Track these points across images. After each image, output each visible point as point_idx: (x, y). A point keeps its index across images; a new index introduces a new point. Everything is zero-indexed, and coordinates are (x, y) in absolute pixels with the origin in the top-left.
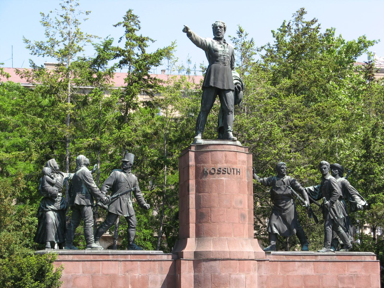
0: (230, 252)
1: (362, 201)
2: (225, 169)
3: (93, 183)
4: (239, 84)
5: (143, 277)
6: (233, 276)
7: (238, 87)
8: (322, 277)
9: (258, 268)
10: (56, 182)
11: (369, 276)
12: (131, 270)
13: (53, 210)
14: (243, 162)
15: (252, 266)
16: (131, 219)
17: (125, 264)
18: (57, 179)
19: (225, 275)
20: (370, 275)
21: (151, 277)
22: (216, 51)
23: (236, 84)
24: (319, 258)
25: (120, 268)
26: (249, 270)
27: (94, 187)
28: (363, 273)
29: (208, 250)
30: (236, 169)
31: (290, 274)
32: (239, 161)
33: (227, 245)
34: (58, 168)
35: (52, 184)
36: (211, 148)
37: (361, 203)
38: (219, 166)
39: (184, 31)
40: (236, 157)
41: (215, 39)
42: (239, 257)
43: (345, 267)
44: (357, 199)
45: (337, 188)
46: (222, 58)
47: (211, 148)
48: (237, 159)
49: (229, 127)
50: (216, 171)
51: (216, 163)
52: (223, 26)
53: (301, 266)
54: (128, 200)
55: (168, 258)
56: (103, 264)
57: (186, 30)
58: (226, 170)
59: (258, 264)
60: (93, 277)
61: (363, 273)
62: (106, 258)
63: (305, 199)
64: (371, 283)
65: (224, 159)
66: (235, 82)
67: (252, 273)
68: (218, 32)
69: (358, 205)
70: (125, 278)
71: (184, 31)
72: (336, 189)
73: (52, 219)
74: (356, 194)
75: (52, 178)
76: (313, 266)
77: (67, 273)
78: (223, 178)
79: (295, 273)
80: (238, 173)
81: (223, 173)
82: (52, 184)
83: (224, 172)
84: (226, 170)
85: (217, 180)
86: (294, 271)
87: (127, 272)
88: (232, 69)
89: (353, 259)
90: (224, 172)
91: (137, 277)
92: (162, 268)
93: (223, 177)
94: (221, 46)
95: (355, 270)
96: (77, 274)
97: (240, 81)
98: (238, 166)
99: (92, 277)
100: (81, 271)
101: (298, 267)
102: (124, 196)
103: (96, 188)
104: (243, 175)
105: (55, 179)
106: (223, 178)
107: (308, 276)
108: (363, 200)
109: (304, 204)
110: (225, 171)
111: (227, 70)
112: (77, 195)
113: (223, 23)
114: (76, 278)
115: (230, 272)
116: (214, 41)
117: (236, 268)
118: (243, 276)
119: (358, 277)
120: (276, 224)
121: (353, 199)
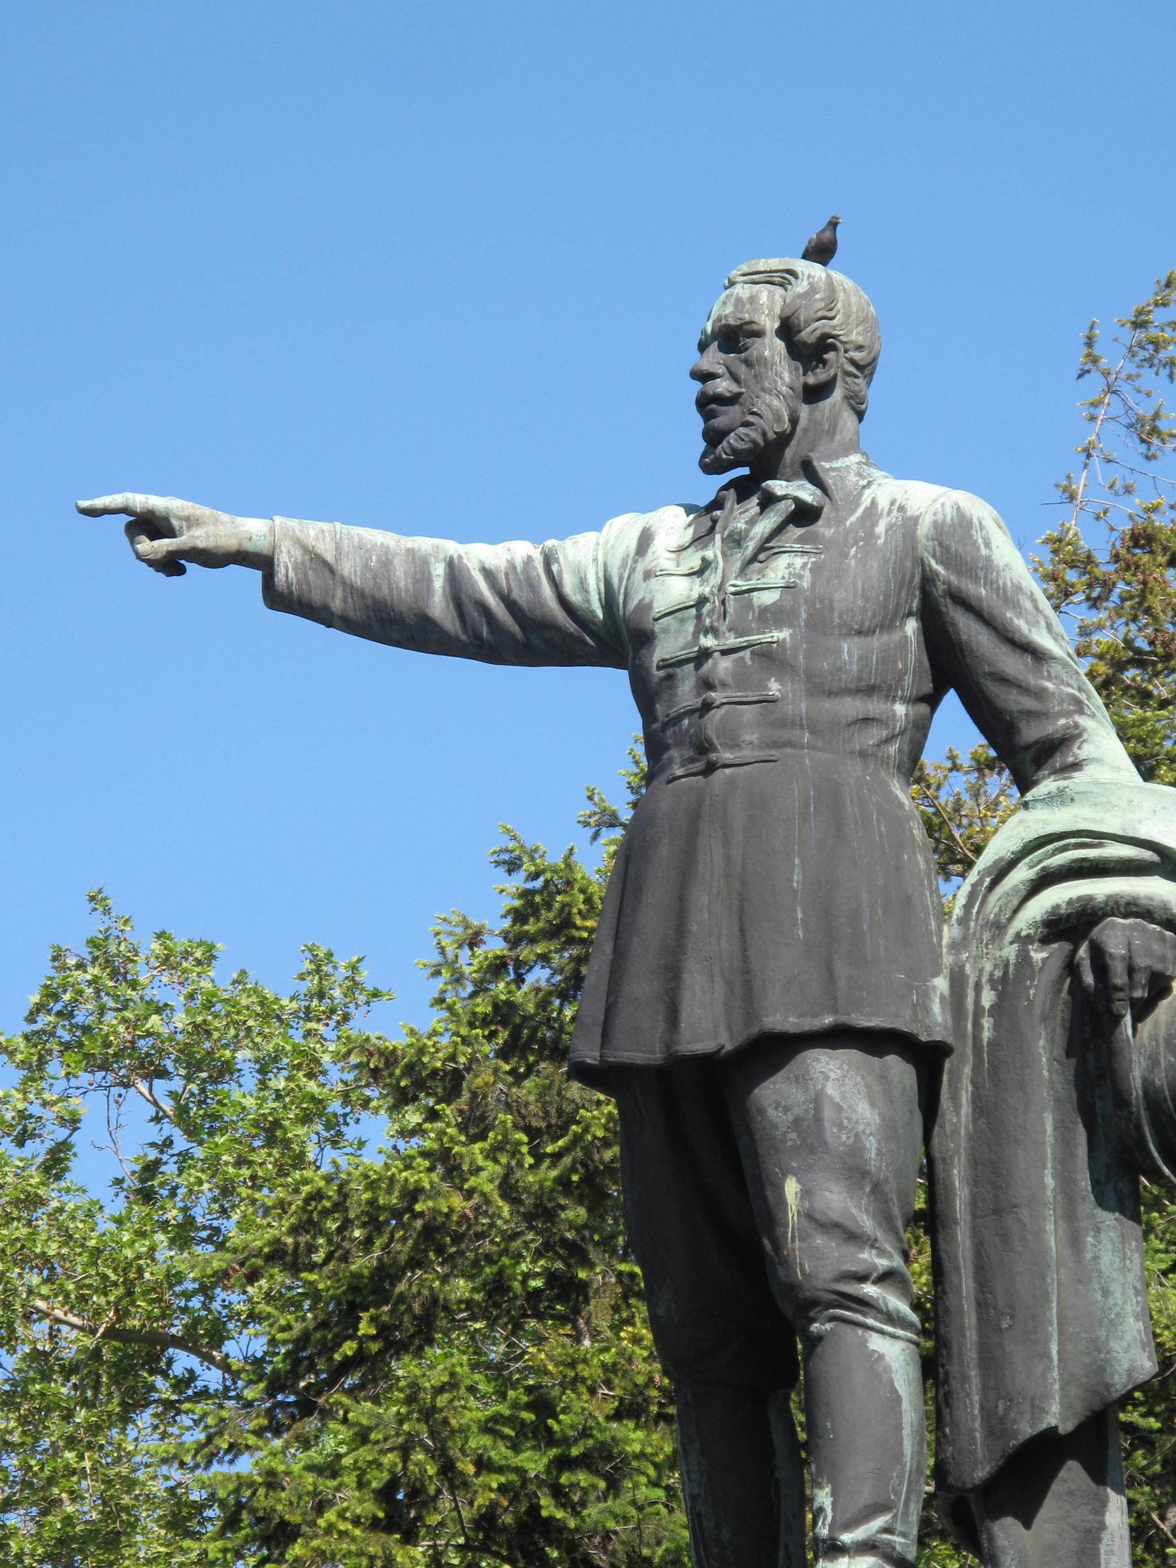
46: (686, 693)
111: (738, 816)
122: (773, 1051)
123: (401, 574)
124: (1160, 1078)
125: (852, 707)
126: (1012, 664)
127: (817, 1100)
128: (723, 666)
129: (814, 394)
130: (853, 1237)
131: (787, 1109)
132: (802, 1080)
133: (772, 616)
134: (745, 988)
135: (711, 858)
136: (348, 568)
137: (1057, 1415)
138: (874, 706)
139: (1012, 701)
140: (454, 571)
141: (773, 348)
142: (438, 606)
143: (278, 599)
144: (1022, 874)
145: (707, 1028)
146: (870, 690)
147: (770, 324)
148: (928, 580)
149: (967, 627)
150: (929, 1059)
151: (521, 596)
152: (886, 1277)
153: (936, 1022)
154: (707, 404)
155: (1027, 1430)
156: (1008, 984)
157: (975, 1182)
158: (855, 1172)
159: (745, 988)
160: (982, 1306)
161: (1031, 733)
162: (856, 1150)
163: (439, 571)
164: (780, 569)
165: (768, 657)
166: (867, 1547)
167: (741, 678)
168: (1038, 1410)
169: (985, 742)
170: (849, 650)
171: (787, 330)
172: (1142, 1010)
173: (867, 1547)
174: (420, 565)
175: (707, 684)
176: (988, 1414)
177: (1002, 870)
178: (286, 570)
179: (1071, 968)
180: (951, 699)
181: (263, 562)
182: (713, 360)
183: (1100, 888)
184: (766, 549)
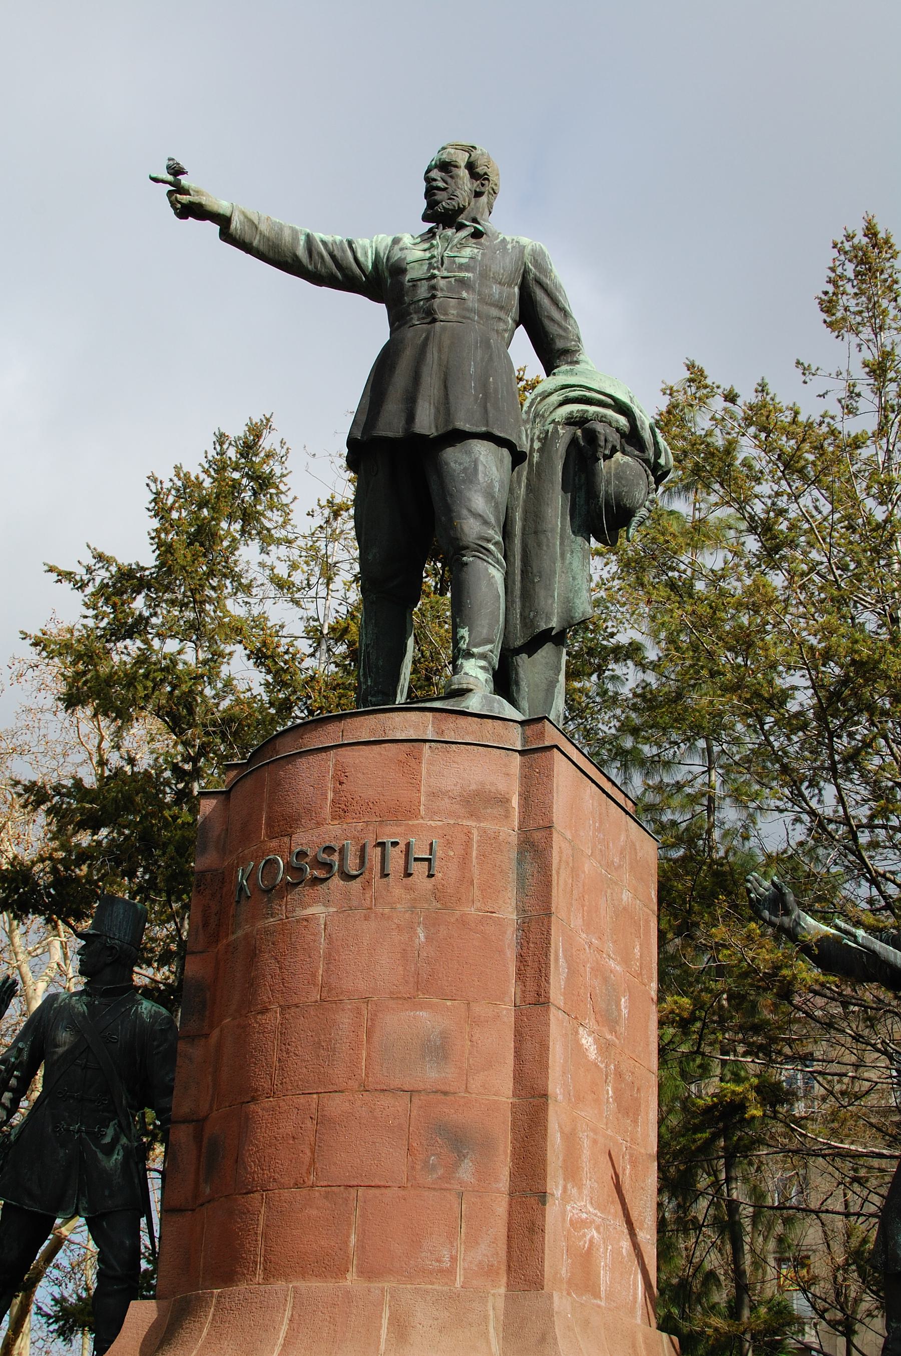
2: (329, 849)
30: (402, 846)
33: (284, 1327)
46: (423, 291)
48: (414, 784)
58: (336, 857)
65: (330, 795)
78: (309, 911)
80: (420, 869)
81: (316, 881)
93: (315, 901)
104: (465, 880)
106: (316, 910)
110: (328, 866)
111: (446, 342)
122: (457, 437)
123: (287, 235)
124: (612, 490)
125: (494, 312)
126: (556, 315)
127: (476, 462)
128: (442, 283)
129: (478, 194)
130: (486, 522)
131: (460, 464)
132: (469, 453)
133: (461, 267)
134: (445, 407)
135: (432, 356)
136: (263, 227)
137: (554, 623)
138: (502, 315)
139: (553, 329)
140: (309, 239)
141: (464, 173)
142: (301, 251)
143: (227, 236)
144: (555, 398)
145: (426, 422)
146: (501, 308)
147: (463, 164)
148: (526, 272)
149: (540, 295)
150: (518, 457)
151: (337, 253)
152: (496, 544)
153: (524, 445)
154: (430, 192)
155: (543, 626)
156: (546, 440)
157: (525, 520)
158: (489, 495)
159: (445, 407)
160: (524, 572)
161: (560, 344)
162: (490, 486)
163: (302, 238)
164: (467, 252)
165: (462, 282)
166: (483, 656)
167: (450, 288)
168: (548, 619)
169: (353, 497)
170: (495, 289)
171: (471, 166)
172: (607, 457)
173: (483, 656)
174: (295, 233)
175: (433, 288)
176: (523, 617)
177: (546, 395)
178: (236, 224)
179: (574, 441)
180: (521, 331)
181: (223, 221)
182: (435, 174)
183: (592, 409)
184: (462, 245)
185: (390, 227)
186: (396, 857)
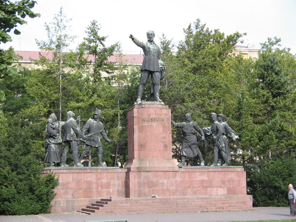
0: (158, 167)
1: (236, 136)
3: (77, 128)
4: (163, 67)
5: (107, 183)
6: (160, 181)
7: (163, 70)
8: (212, 181)
9: (175, 176)
10: (56, 127)
11: (240, 180)
12: (100, 179)
13: (54, 143)
14: (166, 114)
15: (171, 175)
16: (99, 148)
17: (97, 174)
18: (56, 126)
19: (155, 181)
20: (240, 179)
21: (112, 182)
22: (149, 48)
23: (161, 67)
24: (210, 170)
25: (94, 177)
26: (169, 178)
27: (78, 130)
28: (236, 178)
29: (144, 166)
31: (193, 179)
32: (163, 114)
34: (56, 119)
35: (54, 129)
36: (147, 106)
37: (235, 137)
38: (151, 117)
39: (130, 37)
40: (161, 111)
41: (149, 41)
42: (164, 170)
43: (226, 175)
44: (233, 135)
45: (221, 129)
47: (147, 106)
49: (157, 93)
50: (150, 120)
51: (149, 115)
52: (153, 33)
53: (200, 175)
54: (98, 137)
55: (122, 171)
56: (84, 175)
57: (131, 37)
59: (175, 173)
60: (78, 182)
61: (236, 178)
62: (85, 171)
63: (202, 136)
64: (241, 184)
66: (160, 66)
67: (171, 179)
68: (150, 37)
69: (233, 138)
70: (97, 183)
71: (130, 37)
72: (220, 129)
73: (53, 149)
74: (233, 132)
75: (53, 125)
76: (206, 175)
77: (63, 180)
78: (153, 124)
79: (197, 179)
82: (54, 129)
83: (155, 120)
84: (156, 119)
85: (150, 125)
86: (196, 177)
87: (98, 179)
88: (159, 59)
89: (230, 170)
90: (155, 120)
91: (104, 183)
92: (118, 177)
93: (154, 123)
94: (152, 45)
95: (232, 177)
96: (69, 181)
97: (163, 66)
98: (163, 117)
99: (78, 182)
100: (71, 179)
101: (198, 176)
102: (95, 135)
103: (79, 130)
105: (55, 125)
106: (153, 124)
107: (204, 180)
108: (237, 136)
109: (202, 138)
112: (68, 135)
113: (153, 32)
114: (68, 183)
115: (158, 179)
116: (148, 42)
117: (162, 176)
118: (165, 181)
119: (233, 181)
120: (185, 150)
121: (230, 135)
185: (144, 40)
186: (161, 120)
